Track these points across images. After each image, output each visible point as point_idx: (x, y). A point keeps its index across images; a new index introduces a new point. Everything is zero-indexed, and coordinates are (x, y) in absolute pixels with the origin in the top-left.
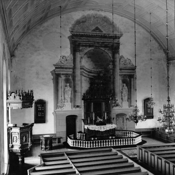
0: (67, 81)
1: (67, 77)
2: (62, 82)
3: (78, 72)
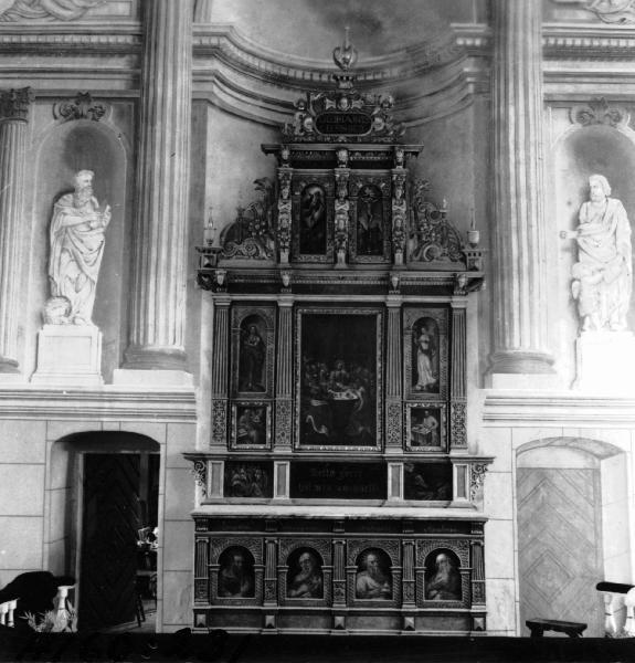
0: (81, 149)
1: (78, 116)
2: (24, 284)
3: (176, 85)
